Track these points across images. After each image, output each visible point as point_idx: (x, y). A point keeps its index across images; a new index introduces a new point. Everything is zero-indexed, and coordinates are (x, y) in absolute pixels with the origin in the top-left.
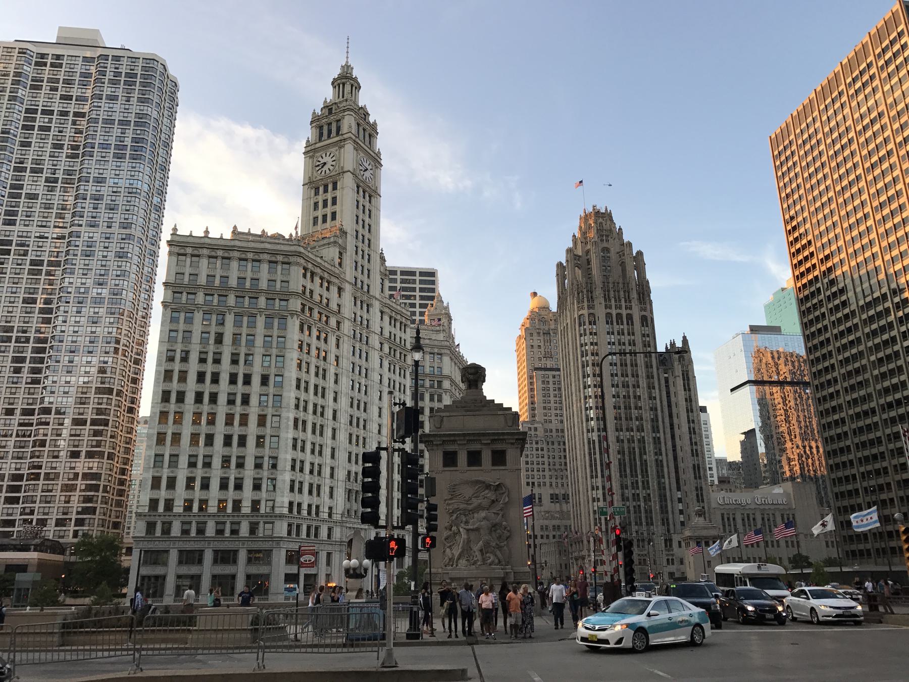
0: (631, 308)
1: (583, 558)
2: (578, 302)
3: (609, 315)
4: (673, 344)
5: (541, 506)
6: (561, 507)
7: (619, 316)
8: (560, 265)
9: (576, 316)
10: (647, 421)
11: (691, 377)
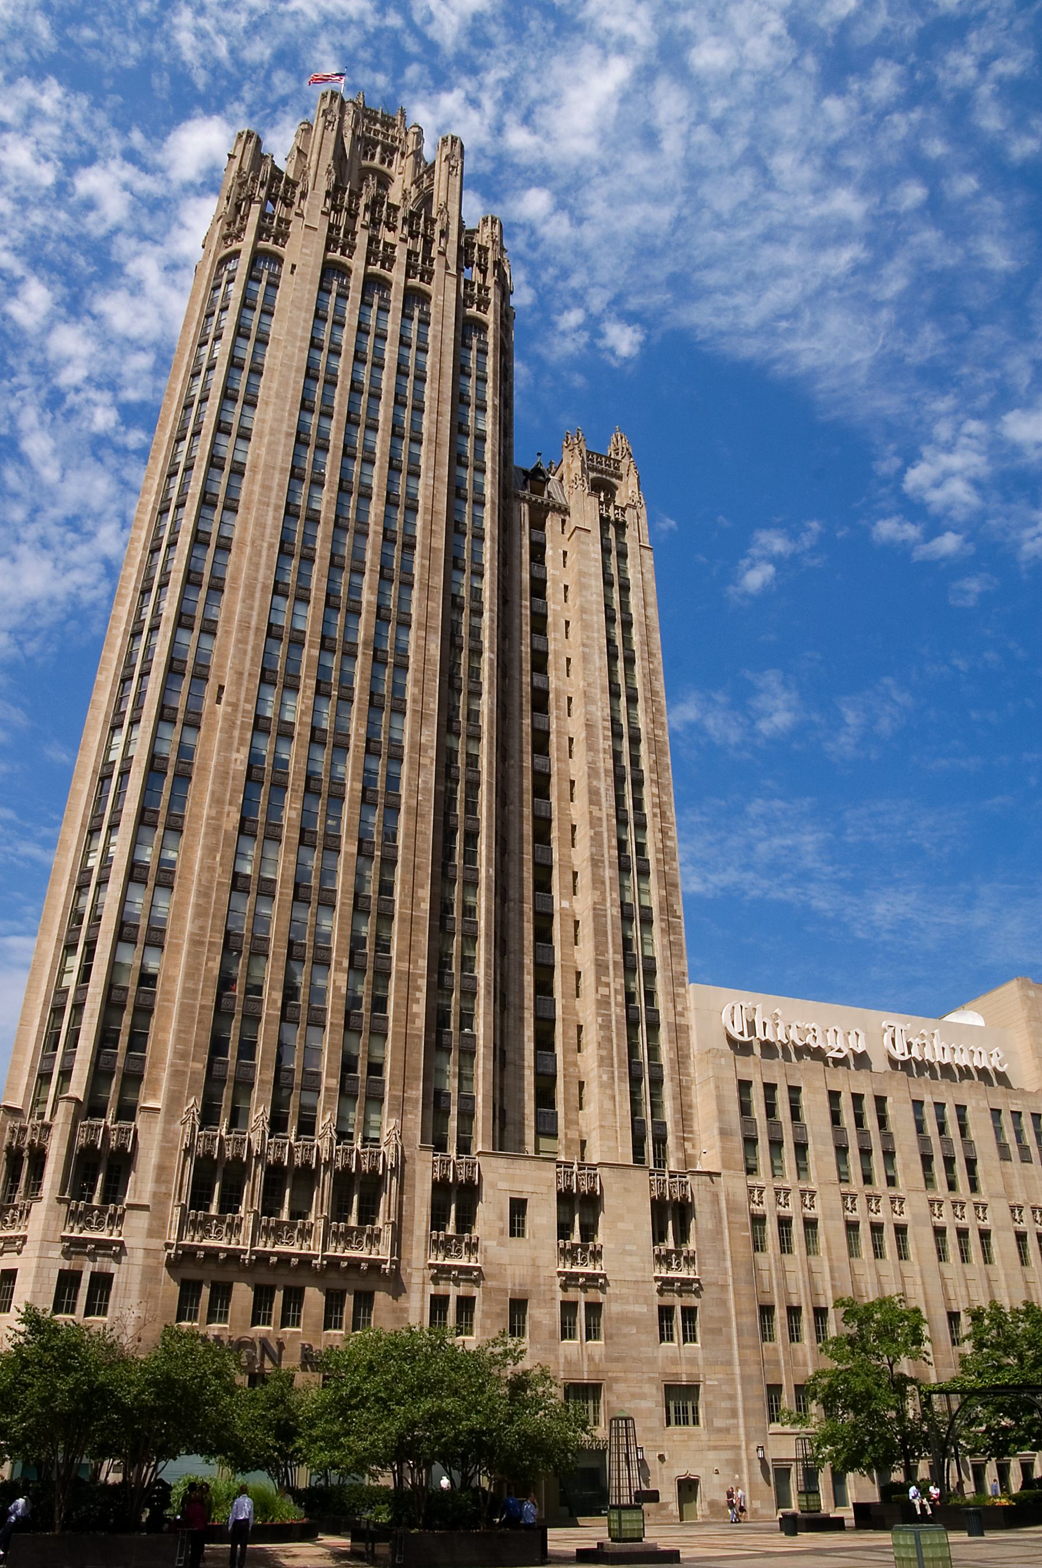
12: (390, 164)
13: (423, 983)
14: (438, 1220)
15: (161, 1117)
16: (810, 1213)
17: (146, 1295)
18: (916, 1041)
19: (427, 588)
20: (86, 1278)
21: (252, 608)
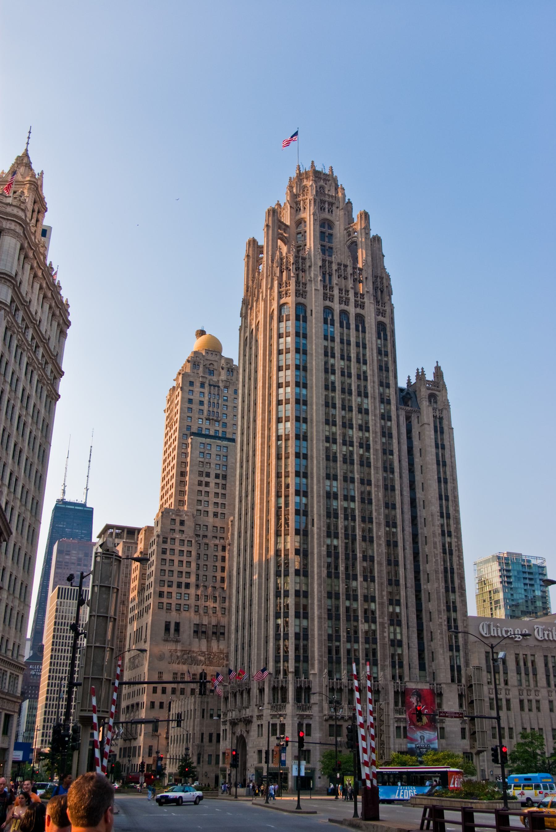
0: (362, 306)
1: (248, 721)
2: (280, 285)
3: (328, 310)
4: (420, 376)
5: (177, 641)
6: (209, 647)
7: (344, 313)
8: (253, 243)
9: (275, 306)
10: (377, 486)
11: (446, 428)
12: (332, 211)
13: (386, 625)
14: (396, 704)
15: (317, 676)
16: (508, 697)
17: (321, 730)
18: (546, 633)
19: (376, 468)
20: (304, 725)
21: (320, 487)
